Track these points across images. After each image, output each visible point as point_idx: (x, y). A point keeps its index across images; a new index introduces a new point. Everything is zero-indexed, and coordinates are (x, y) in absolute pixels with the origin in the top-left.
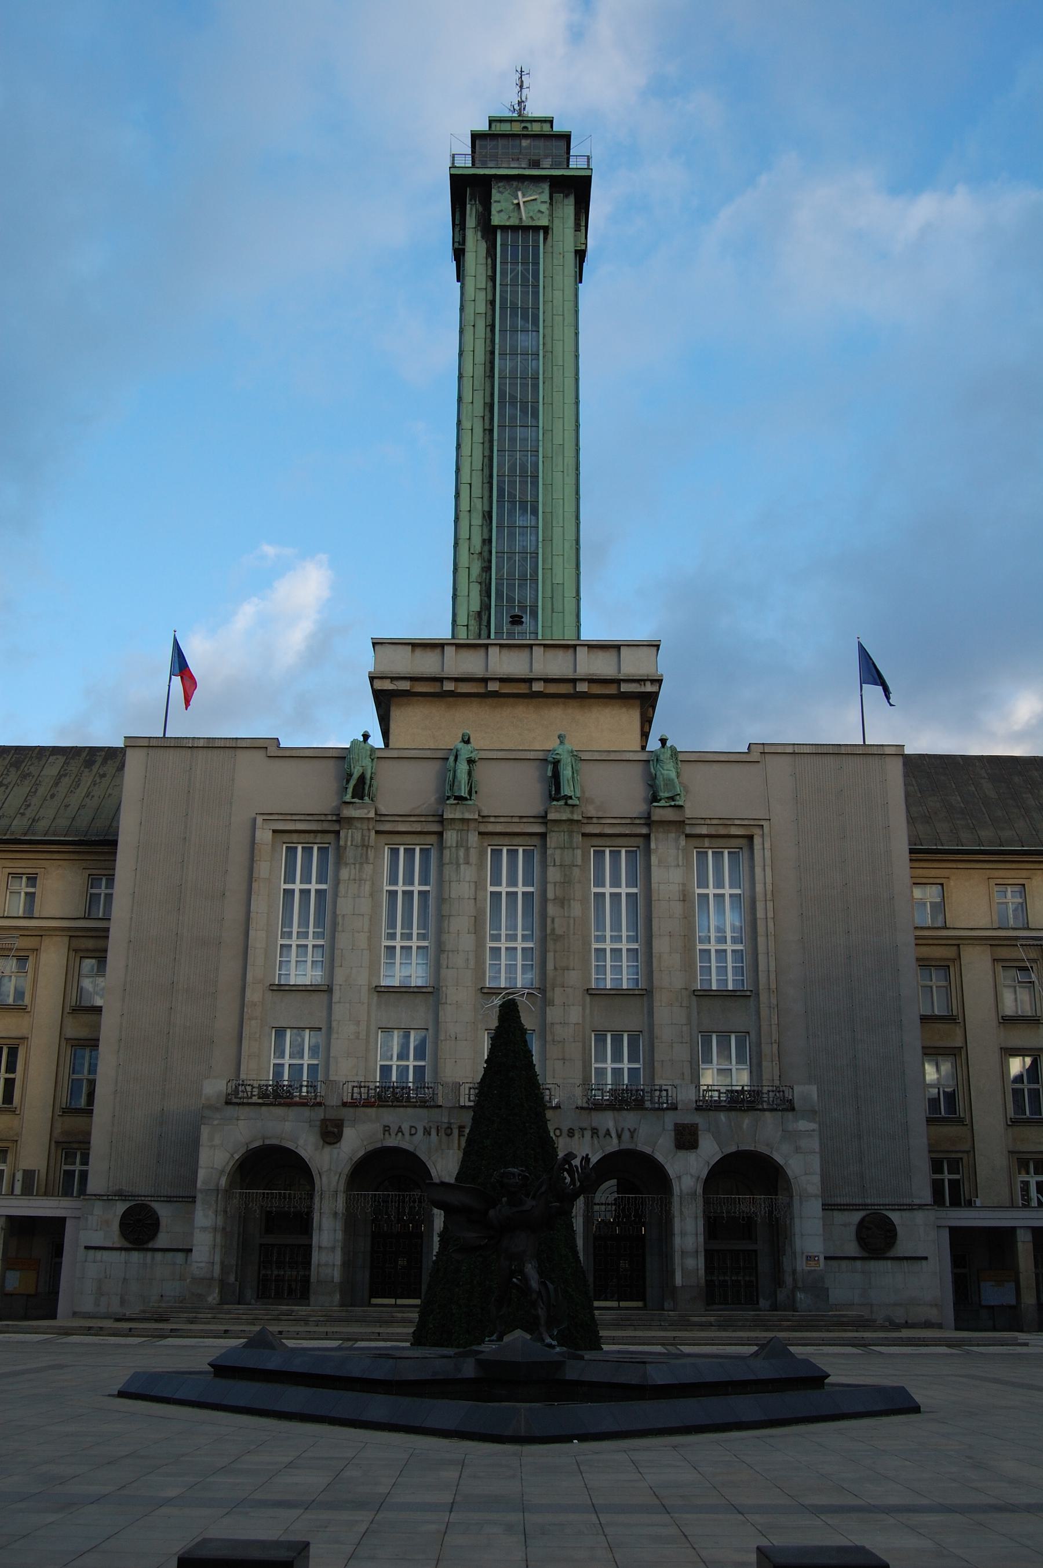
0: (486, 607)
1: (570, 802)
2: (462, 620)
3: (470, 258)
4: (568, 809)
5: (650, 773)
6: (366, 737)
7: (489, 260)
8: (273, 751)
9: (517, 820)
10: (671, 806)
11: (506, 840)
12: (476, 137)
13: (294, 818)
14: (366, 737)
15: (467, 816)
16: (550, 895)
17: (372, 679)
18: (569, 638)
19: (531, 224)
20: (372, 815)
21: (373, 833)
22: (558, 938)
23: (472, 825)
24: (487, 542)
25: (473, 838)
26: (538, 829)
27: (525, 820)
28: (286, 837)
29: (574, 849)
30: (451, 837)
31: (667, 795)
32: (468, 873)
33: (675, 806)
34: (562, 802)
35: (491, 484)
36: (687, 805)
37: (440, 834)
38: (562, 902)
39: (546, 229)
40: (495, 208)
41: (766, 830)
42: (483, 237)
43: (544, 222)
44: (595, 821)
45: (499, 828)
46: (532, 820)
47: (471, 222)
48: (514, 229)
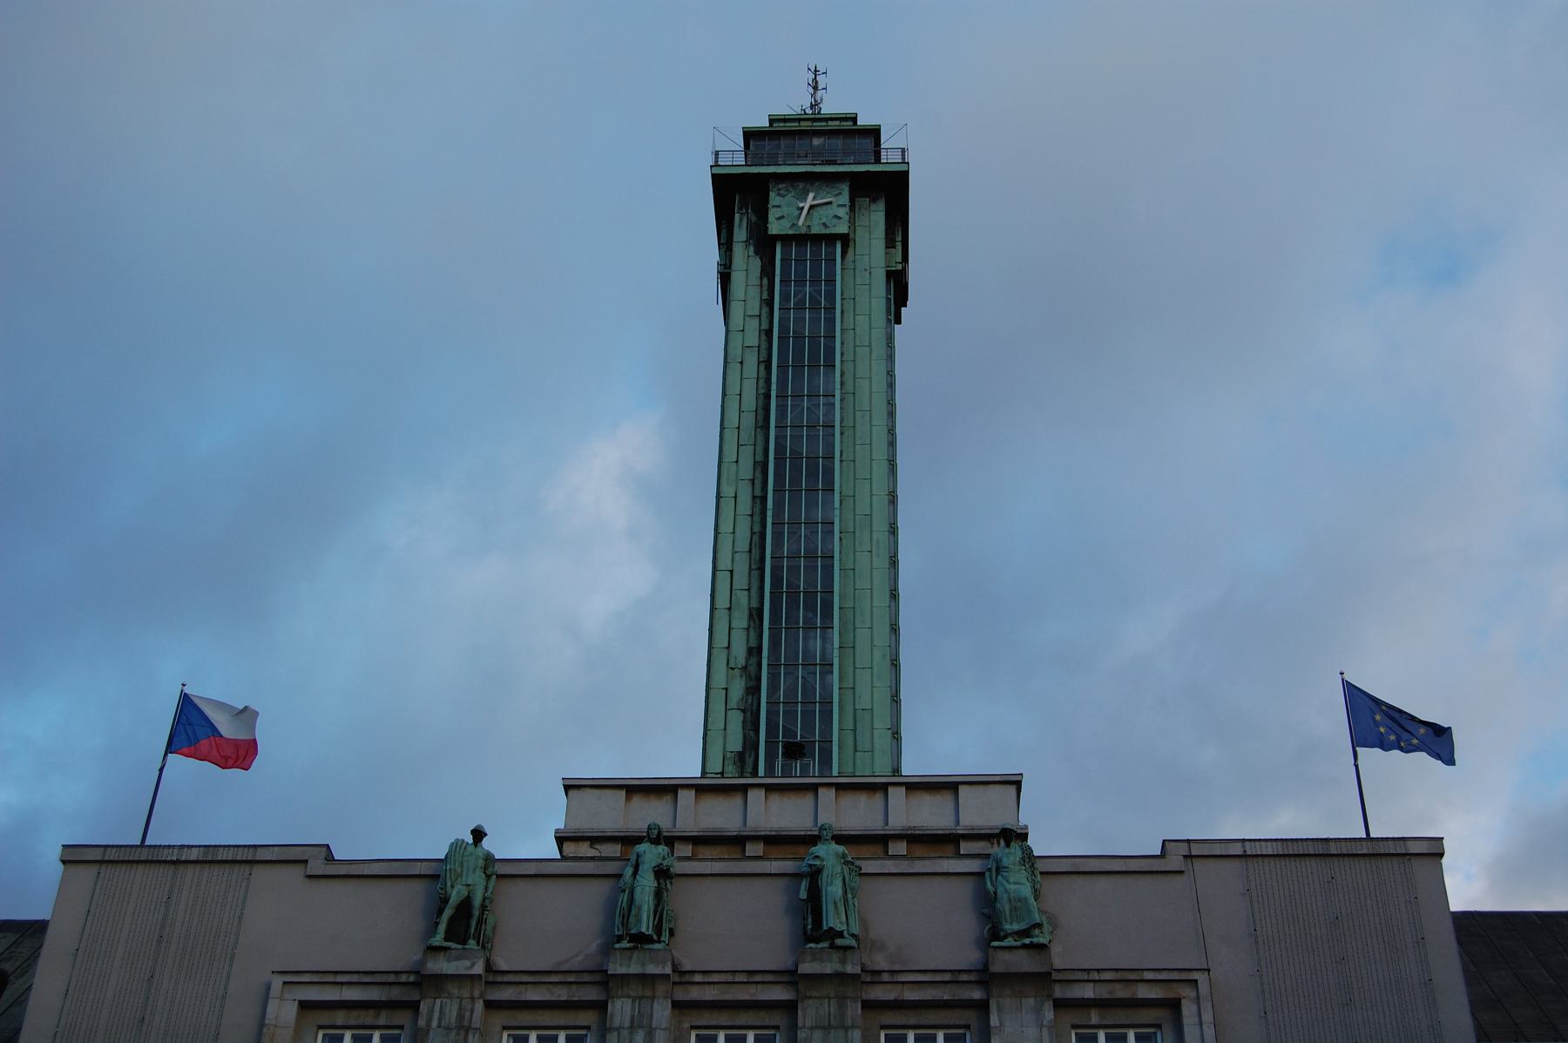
1: (839, 942)
3: (738, 278)
4: (836, 955)
5: (987, 893)
6: (478, 834)
7: (765, 281)
8: (317, 866)
9: (742, 978)
10: (1024, 946)
11: (723, 1018)
12: (750, 135)
13: (340, 979)
14: (478, 834)
15: (651, 969)
18: (879, 770)
19: (823, 231)
20: (479, 969)
21: (479, 1005)
23: (661, 988)
25: (662, 1012)
26: (779, 994)
27: (758, 978)
28: (324, 1017)
29: (846, 1029)
30: (621, 1010)
31: (1016, 927)
33: (1032, 946)
34: (825, 944)
36: (1056, 949)
37: (601, 1007)
39: (846, 240)
40: (773, 214)
41: (1203, 988)
42: (756, 253)
43: (842, 229)
44: (886, 977)
45: (710, 994)
46: (770, 978)
47: (740, 234)
48: (802, 239)
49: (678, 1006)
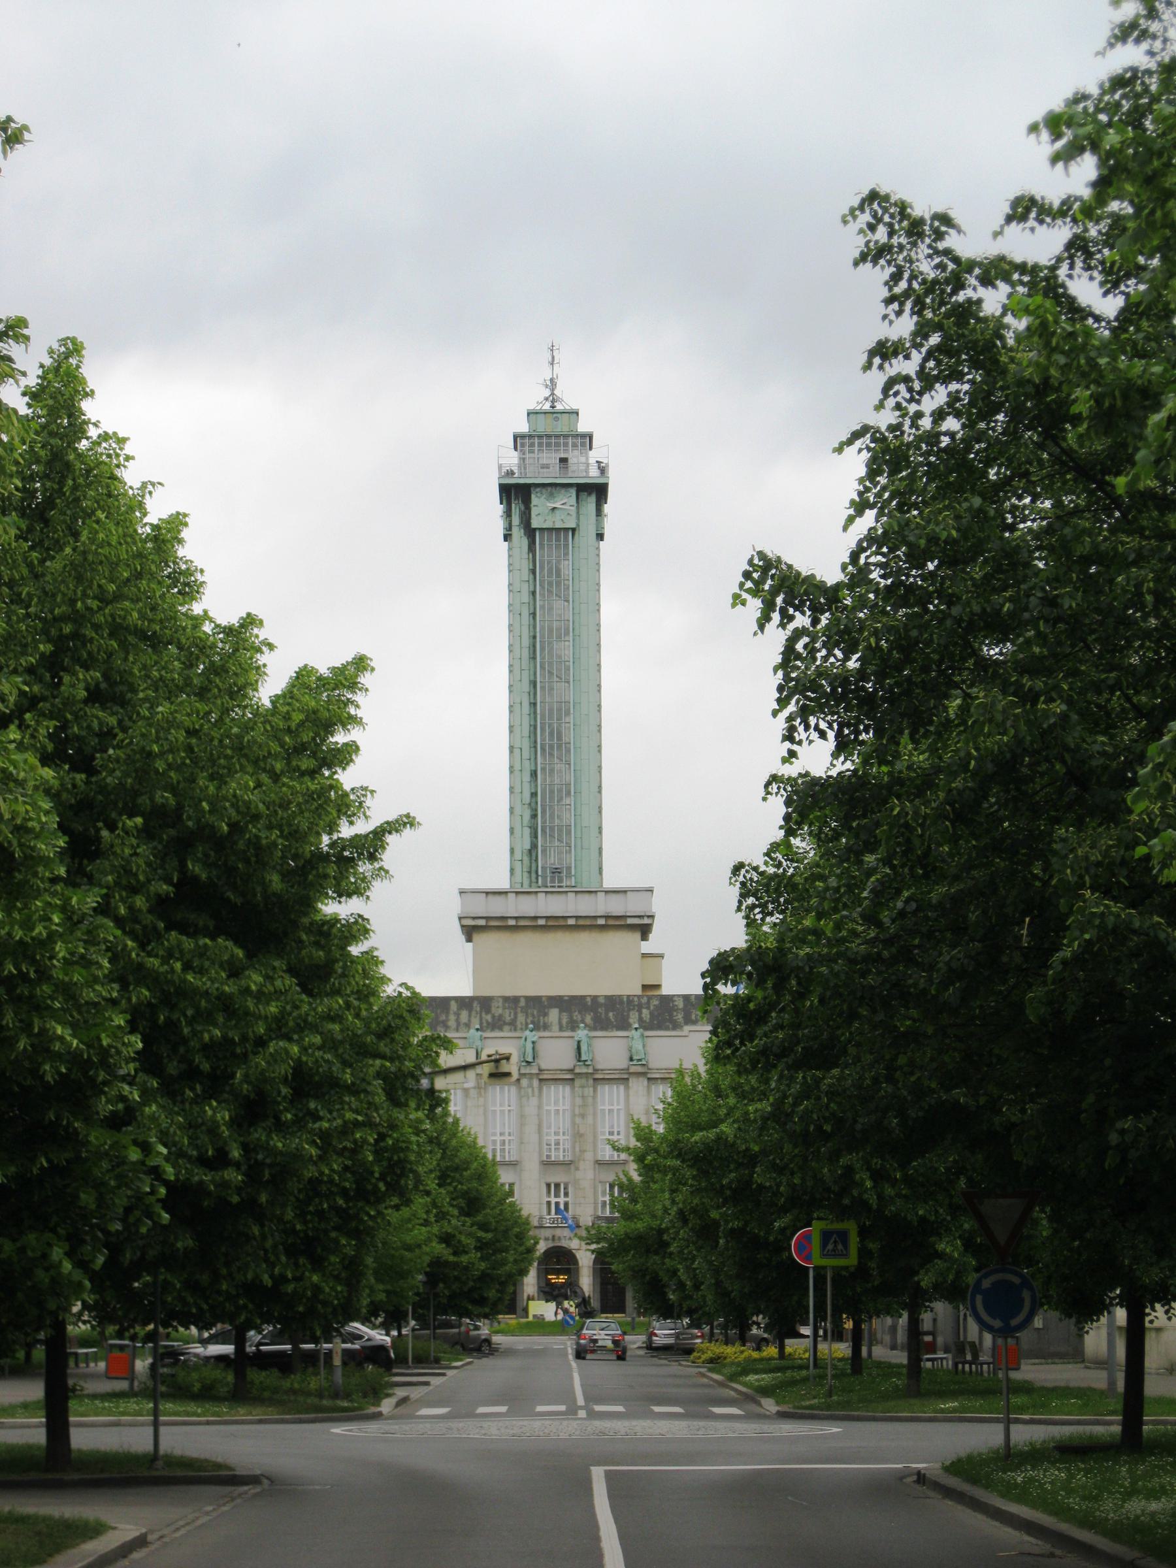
0: (534, 846)
2: (518, 856)
16: (577, 1112)
17: (460, 918)
22: (581, 1135)
24: (534, 795)
25: (536, 1083)
30: (524, 1082)
32: (534, 1101)
35: (535, 747)
38: (583, 1116)
39: (574, 530)
40: (534, 512)
48: (550, 530)
49: (541, 1080)
